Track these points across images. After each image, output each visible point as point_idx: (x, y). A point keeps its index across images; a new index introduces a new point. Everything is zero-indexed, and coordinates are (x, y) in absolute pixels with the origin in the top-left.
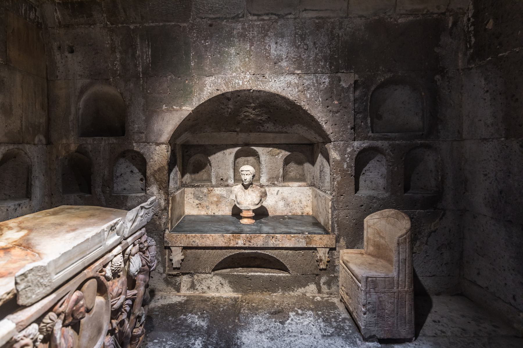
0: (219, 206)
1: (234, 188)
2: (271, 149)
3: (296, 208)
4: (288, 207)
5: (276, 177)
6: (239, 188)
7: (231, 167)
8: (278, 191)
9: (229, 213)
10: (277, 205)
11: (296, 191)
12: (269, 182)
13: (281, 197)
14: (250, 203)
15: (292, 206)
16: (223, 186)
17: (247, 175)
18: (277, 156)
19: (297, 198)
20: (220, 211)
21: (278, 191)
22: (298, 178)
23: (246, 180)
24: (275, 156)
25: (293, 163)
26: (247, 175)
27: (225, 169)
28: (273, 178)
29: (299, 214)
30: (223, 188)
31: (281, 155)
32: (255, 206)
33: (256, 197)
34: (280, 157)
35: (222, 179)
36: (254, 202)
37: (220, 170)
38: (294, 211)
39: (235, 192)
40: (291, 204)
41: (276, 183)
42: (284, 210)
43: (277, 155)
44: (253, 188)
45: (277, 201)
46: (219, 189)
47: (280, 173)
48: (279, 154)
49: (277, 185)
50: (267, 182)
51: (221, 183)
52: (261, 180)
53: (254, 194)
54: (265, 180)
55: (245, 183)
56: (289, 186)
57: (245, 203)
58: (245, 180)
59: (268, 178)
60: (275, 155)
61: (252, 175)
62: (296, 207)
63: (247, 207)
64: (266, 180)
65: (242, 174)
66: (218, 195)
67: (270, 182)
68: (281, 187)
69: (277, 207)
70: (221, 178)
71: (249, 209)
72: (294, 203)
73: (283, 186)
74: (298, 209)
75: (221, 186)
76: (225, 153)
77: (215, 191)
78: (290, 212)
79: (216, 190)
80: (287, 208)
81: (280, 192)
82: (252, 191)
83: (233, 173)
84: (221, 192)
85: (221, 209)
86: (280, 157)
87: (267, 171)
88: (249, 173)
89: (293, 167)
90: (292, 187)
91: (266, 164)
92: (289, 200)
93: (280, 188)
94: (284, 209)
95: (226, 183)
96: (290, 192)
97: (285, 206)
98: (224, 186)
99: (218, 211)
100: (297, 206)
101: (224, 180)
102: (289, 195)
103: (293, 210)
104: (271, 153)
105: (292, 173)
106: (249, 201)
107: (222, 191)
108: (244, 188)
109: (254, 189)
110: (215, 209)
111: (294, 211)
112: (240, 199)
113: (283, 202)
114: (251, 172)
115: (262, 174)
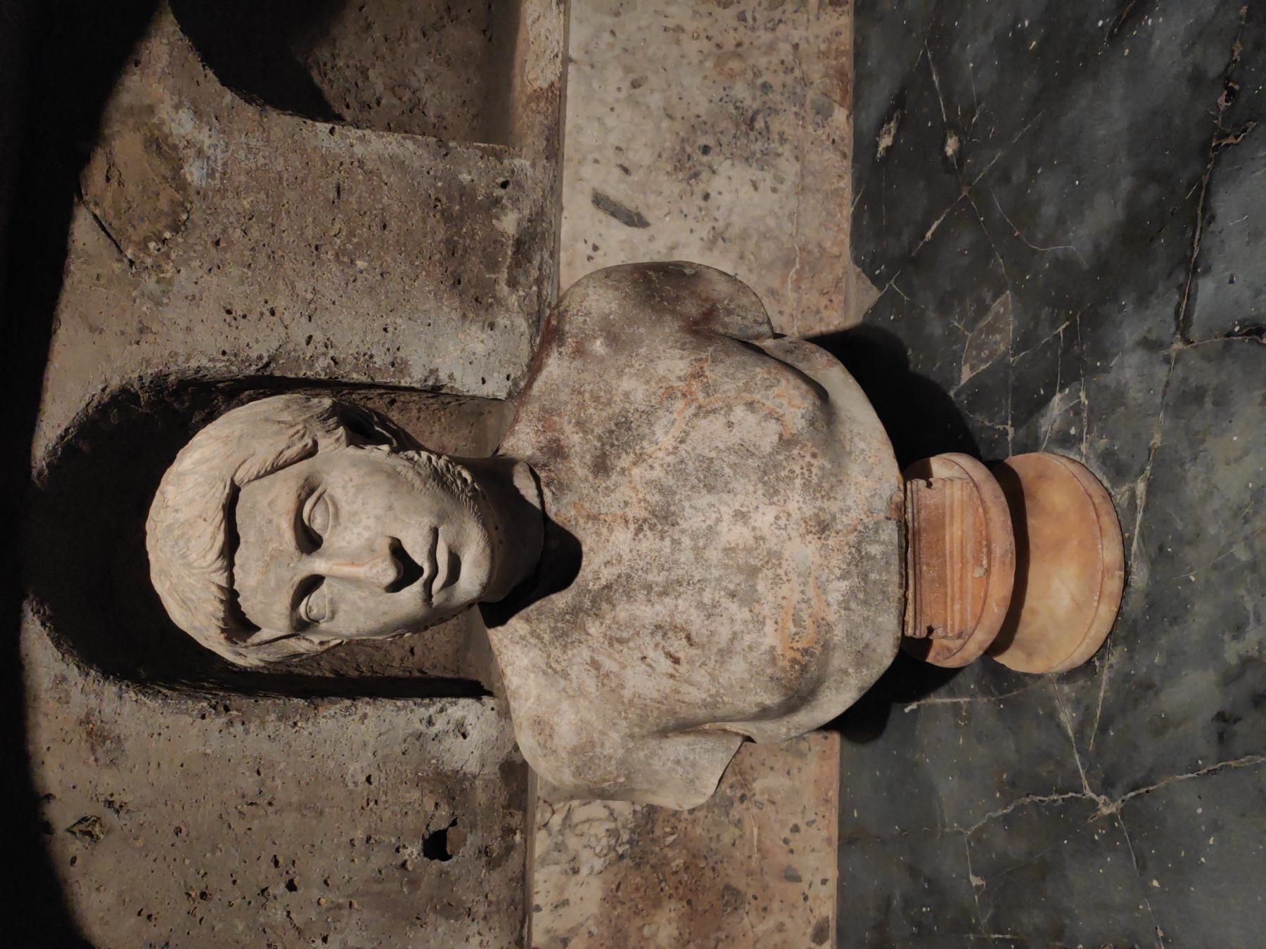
0: (740, 882)
1: (547, 748)
2: (83, 231)
3: (785, 49)
4: (775, 127)
5: (448, 218)
6: (553, 672)
7: (285, 731)
8: (600, 201)
9: (823, 755)
10: (744, 236)
11: (609, 20)
12: (499, 301)
13: (672, 187)
14: (798, 504)
15: (766, 87)
16: (509, 831)
17: (309, 541)
18: (194, 173)
19: (690, 26)
20: (794, 861)
21: (600, 201)
22: (475, 41)
23: (419, 556)
24: (182, 185)
25: (324, 54)
26: (309, 541)
27: (302, 807)
28: (451, 249)
29: (847, 39)
30: (541, 842)
31: (182, 125)
32: (845, 429)
33: (703, 413)
34: (205, 138)
35: (436, 846)
36: (786, 442)
37: (313, 870)
38: (816, 77)
39: (613, 744)
40: (741, 91)
41: (509, 223)
42: (797, 166)
43: (177, 169)
44: (556, 451)
45: (704, 231)
46: (544, 883)
47: (400, 165)
48: (158, 144)
49: (538, 216)
50: (502, 321)
51: (485, 851)
52: (467, 383)
53: (663, 437)
54: (477, 341)
55: (471, 580)
56: (555, 96)
57: (791, 591)
58: (406, 571)
59: (448, 309)
60: (168, 194)
61: (333, 444)
62: (771, 48)
63: (859, 560)
64: (474, 329)
65: (302, 626)
66: (612, 898)
67: (503, 289)
68: (557, 178)
69: (765, 236)
70: (413, 851)
71: (890, 533)
72: (735, 65)
73: (553, 151)
74: (796, 36)
75: (510, 849)
76: (91, 810)
77: (574, 931)
78: (823, 113)
79: (562, 926)
80: (783, 139)
81: (618, 190)
82: (601, 466)
83: (364, 706)
84: (591, 862)
85: (781, 858)
86: (205, 138)
87: (367, 303)
88: (283, 489)
89: (364, 72)
90: (567, 60)
91: (281, 303)
92: (703, 107)
93: (567, 174)
94: (789, 168)
95: (481, 797)
96: (615, 77)
97: (765, 160)
98: (516, 820)
99: (793, 890)
100: (764, 37)
101: (440, 822)
102: (655, 100)
103: (805, 82)
104: (145, 228)
105: (427, 93)
106: (765, 518)
107: (573, 842)
108: (561, 600)
109: (573, 439)
110: (771, 923)
111: (816, 72)
112: (737, 668)
113: (725, 167)
114: (264, 453)
115: (398, 365)
